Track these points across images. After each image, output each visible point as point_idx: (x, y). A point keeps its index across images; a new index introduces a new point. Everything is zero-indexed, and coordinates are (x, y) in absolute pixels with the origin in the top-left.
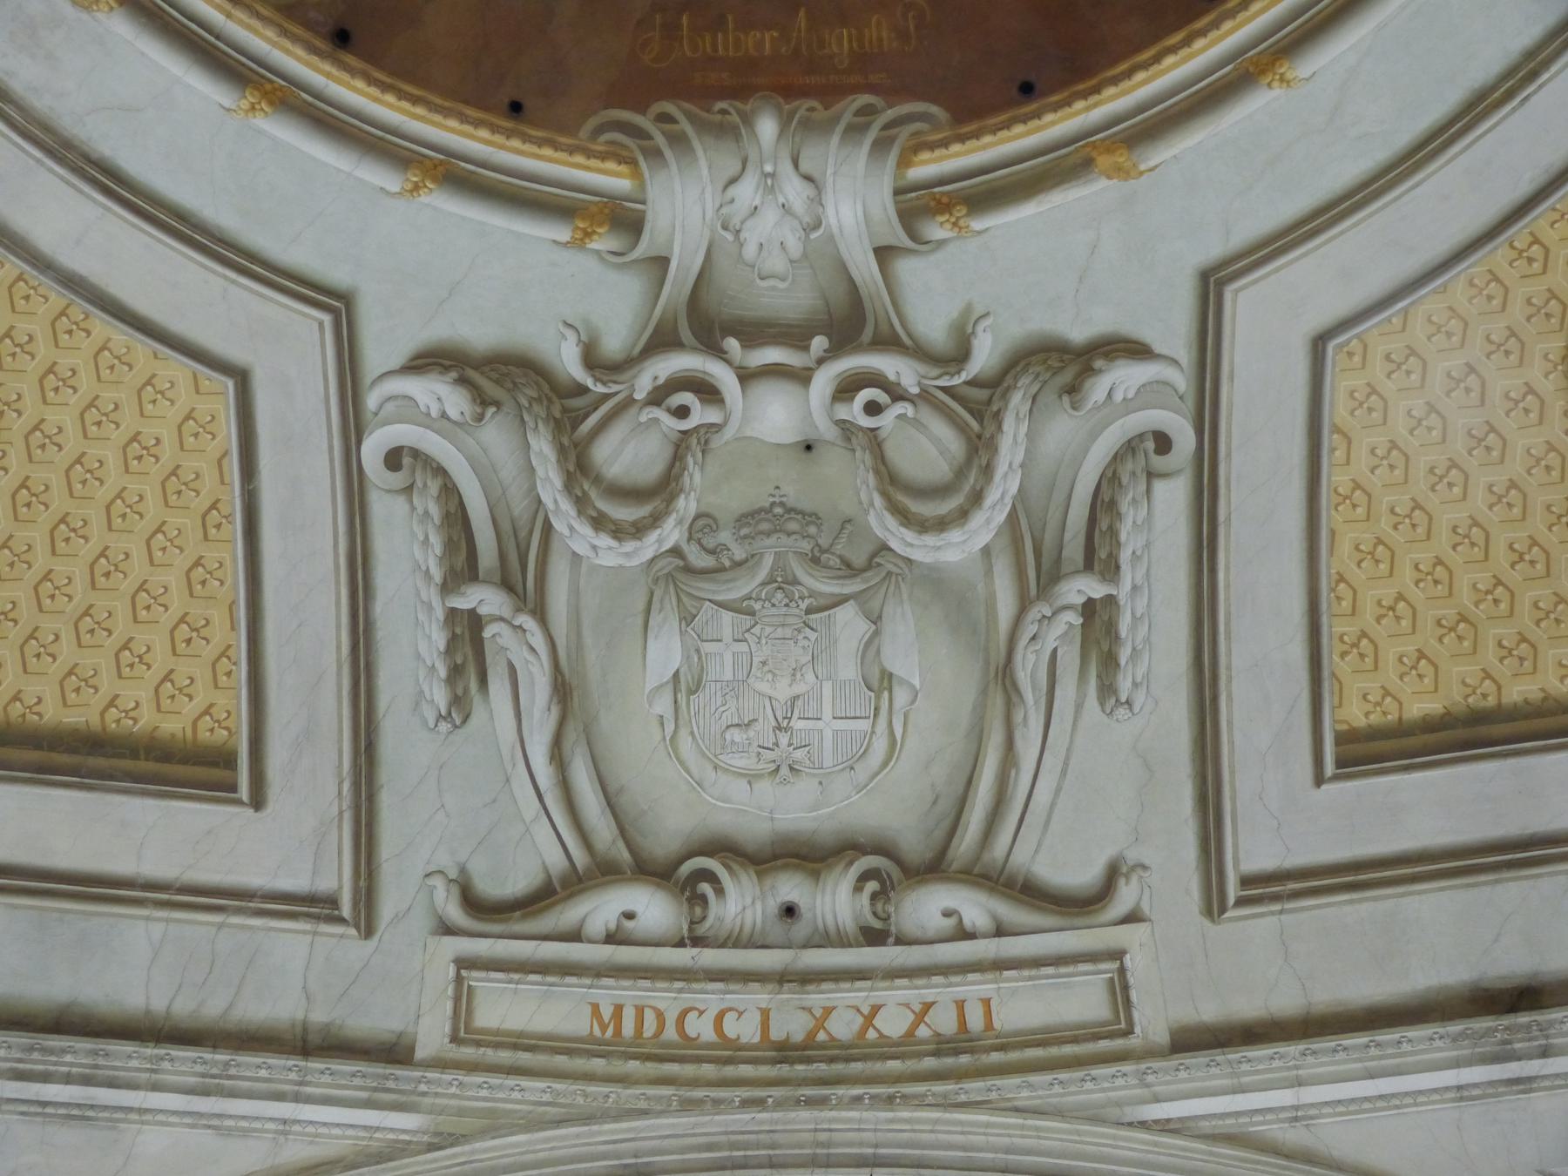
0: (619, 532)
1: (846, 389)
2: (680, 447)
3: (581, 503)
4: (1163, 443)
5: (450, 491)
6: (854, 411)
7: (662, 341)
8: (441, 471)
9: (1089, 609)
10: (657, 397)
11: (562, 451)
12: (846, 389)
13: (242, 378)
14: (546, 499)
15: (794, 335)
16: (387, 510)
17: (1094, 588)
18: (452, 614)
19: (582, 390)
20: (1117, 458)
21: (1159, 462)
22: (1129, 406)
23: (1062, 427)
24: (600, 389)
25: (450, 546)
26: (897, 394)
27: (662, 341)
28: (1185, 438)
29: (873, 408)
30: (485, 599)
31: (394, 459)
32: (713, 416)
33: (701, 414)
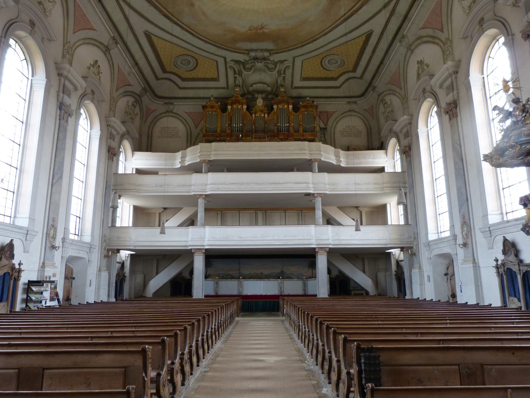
0: (247, 71)
1: (265, 63)
2: (252, 66)
3: (244, 70)
4: (289, 66)
6: (266, 64)
7: (250, 60)
8: (233, 68)
10: (251, 63)
11: (243, 67)
12: (265, 63)
13: (217, 62)
15: (261, 60)
16: (229, 70)
18: (234, 77)
26: (269, 63)
27: (250, 60)
28: (291, 65)
30: (237, 76)
31: (229, 66)
32: (255, 64)
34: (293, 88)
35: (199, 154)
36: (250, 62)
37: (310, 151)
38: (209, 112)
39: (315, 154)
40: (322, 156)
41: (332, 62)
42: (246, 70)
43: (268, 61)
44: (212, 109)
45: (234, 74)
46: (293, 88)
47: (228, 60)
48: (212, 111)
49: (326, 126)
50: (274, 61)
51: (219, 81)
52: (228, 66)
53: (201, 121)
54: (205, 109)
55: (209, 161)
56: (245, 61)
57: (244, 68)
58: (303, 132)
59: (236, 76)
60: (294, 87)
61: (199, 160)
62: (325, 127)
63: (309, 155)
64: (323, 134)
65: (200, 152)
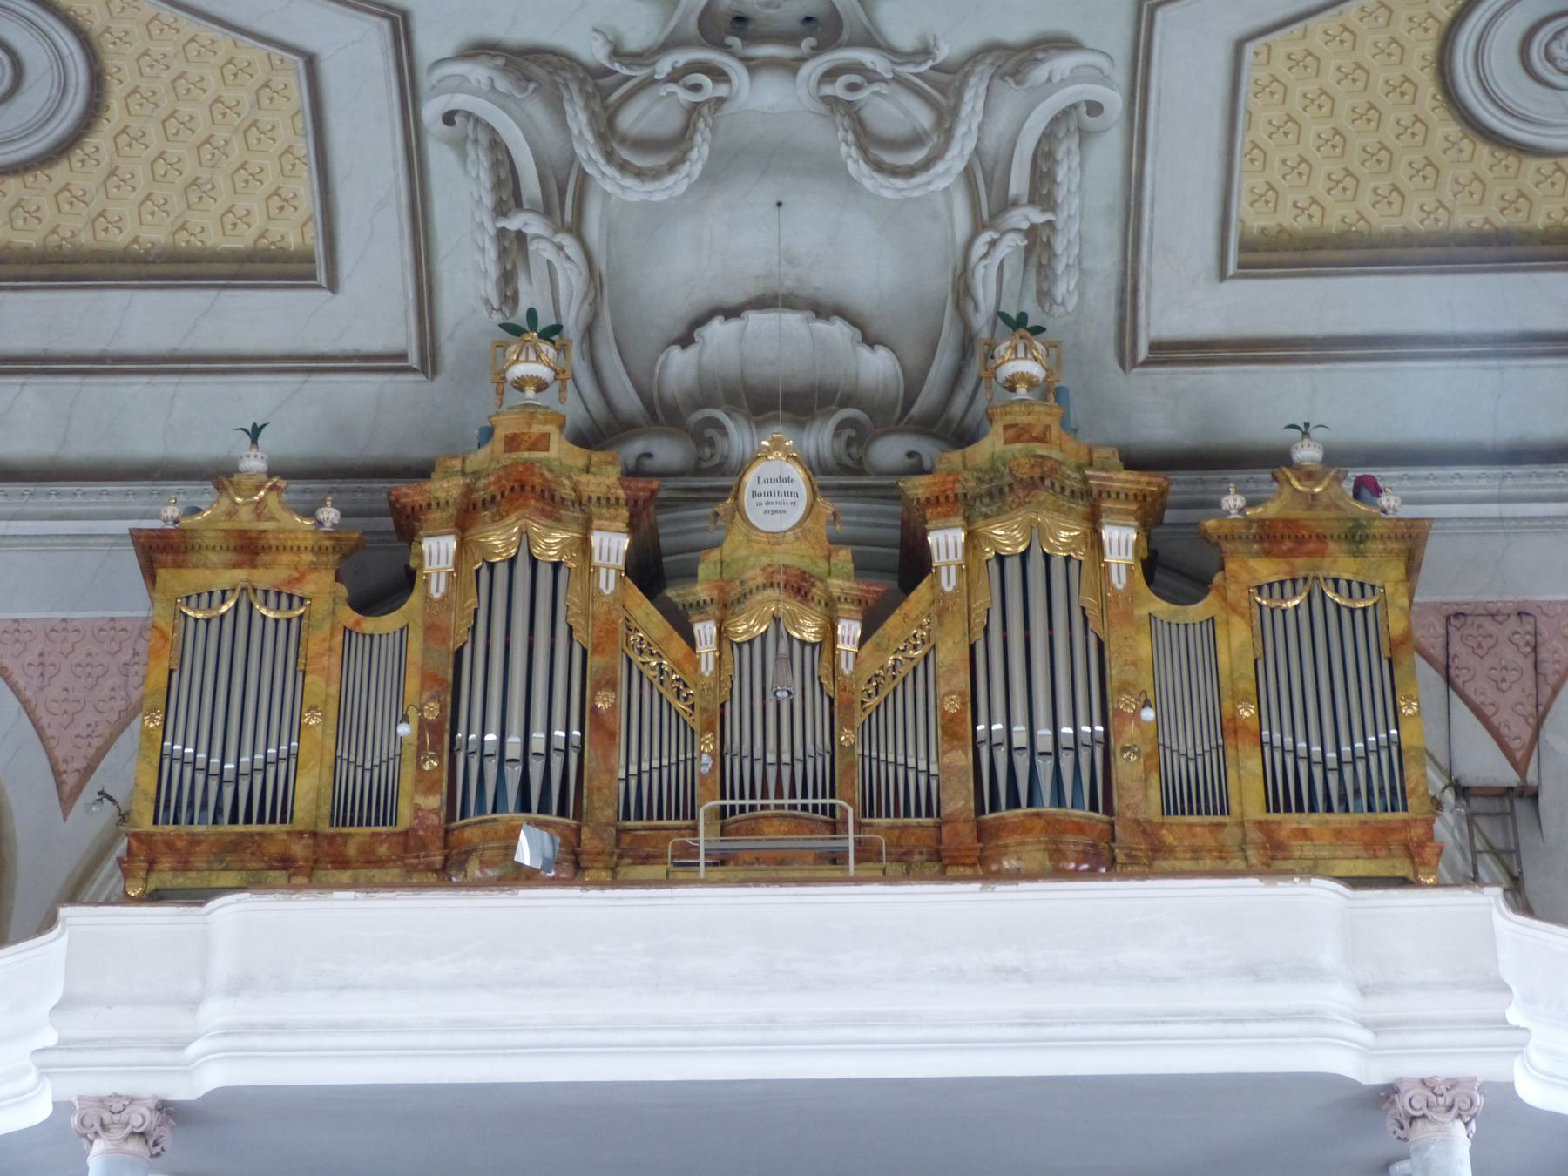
0: (640, 174)
1: (830, 75)
3: (609, 156)
4: (1095, 108)
5: (496, 145)
6: (837, 89)
7: (671, 43)
9: (1032, 232)
10: (675, 77)
11: (593, 117)
12: (830, 75)
14: (580, 151)
17: (1038, 217)
18: (502, 233)
19: (610, 72)
20: (1056, 120)
21: (1091, 122)
22: (1064, 82)
23: (1011, 98)
24: (625, 71)
25: (498, 184)
26: (870, 76)
29: (853, 87)
30: (529, 223)
31: (449, 118)
32: (723, 90)
33: (710, 89)
34: (1143, 352)
35: (50, 1038)
36: (664, 66)
37: (1364, 991)
38: (209, 597)
39: (1432, 1024)
40: (1518, 1049)
41: (1557, 50)
42: (625, 154)
43: (868, 57)
44: (240, 575)
45: (500, 210)
46: (1143, 352)
47: (430, 44)
48: (249, 590)
49: (1520, 767)
50: (925, 52)
51: (333, 286)
52: (431, 111)
53: (122, 725)
54: (162, 574)
55: (165, 1108)
56: (617, 53)
57: (607, 133)
58: (1272, 804)
59: (514, 223)
60: (1156, 346)
61: (38, 1111)
62: (1510, 778)
63: (1366, 1036)
64: (1492, 850)
65: (58, 1007)
